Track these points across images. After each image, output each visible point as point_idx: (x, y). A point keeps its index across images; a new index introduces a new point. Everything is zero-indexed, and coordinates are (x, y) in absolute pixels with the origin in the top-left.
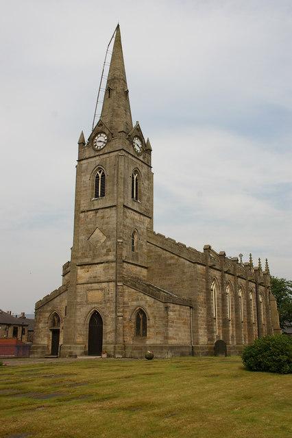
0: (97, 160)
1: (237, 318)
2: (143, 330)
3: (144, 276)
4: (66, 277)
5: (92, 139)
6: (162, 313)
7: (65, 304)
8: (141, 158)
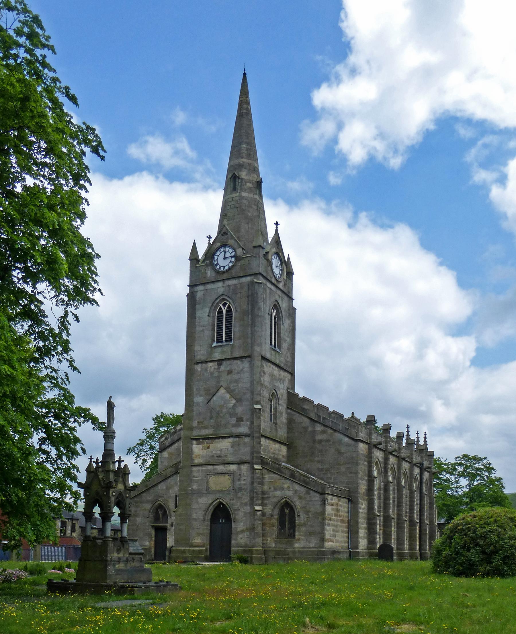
0: (220, 287)
1: (399, 515)
2: (289, 529)
3: (283, 456)
5: (210, 253)
6: (320, 509)
7: (175, 490)
8: (281, 285)
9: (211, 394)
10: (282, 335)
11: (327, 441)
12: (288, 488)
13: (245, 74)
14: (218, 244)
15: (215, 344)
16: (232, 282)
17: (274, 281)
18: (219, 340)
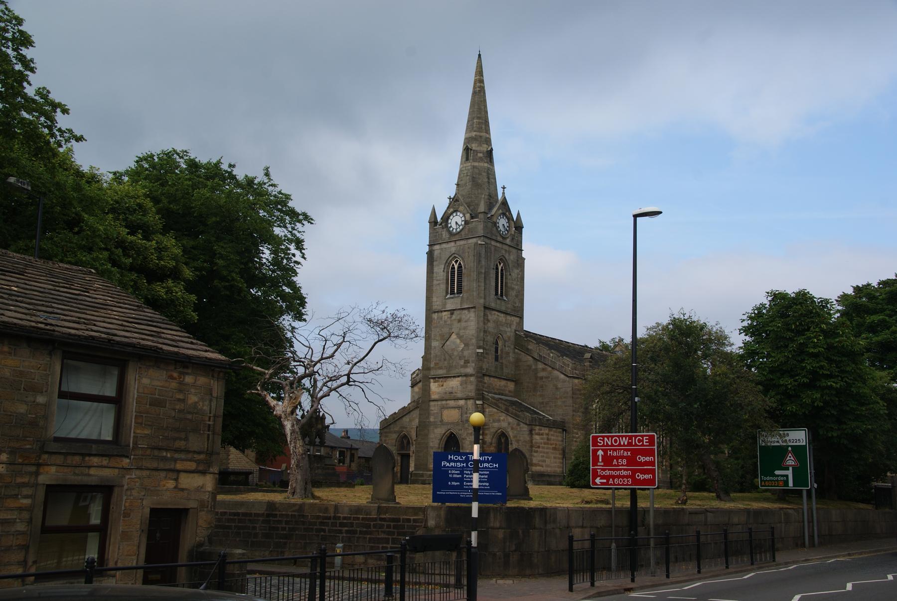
0: (452, 247)
4: (416, 389)
5: (446, 218)
6: (528, 438)
7: (416, 422)
8: (508, 241)
9: (446, 339)
10: (509, 285)
11: (547, 378)
12: (503, 420)
13: (480, 55)
14: (452, 210)
15: (449, 296)
16: (462, 243)
17: (500, 239)
18: (452, 293)
